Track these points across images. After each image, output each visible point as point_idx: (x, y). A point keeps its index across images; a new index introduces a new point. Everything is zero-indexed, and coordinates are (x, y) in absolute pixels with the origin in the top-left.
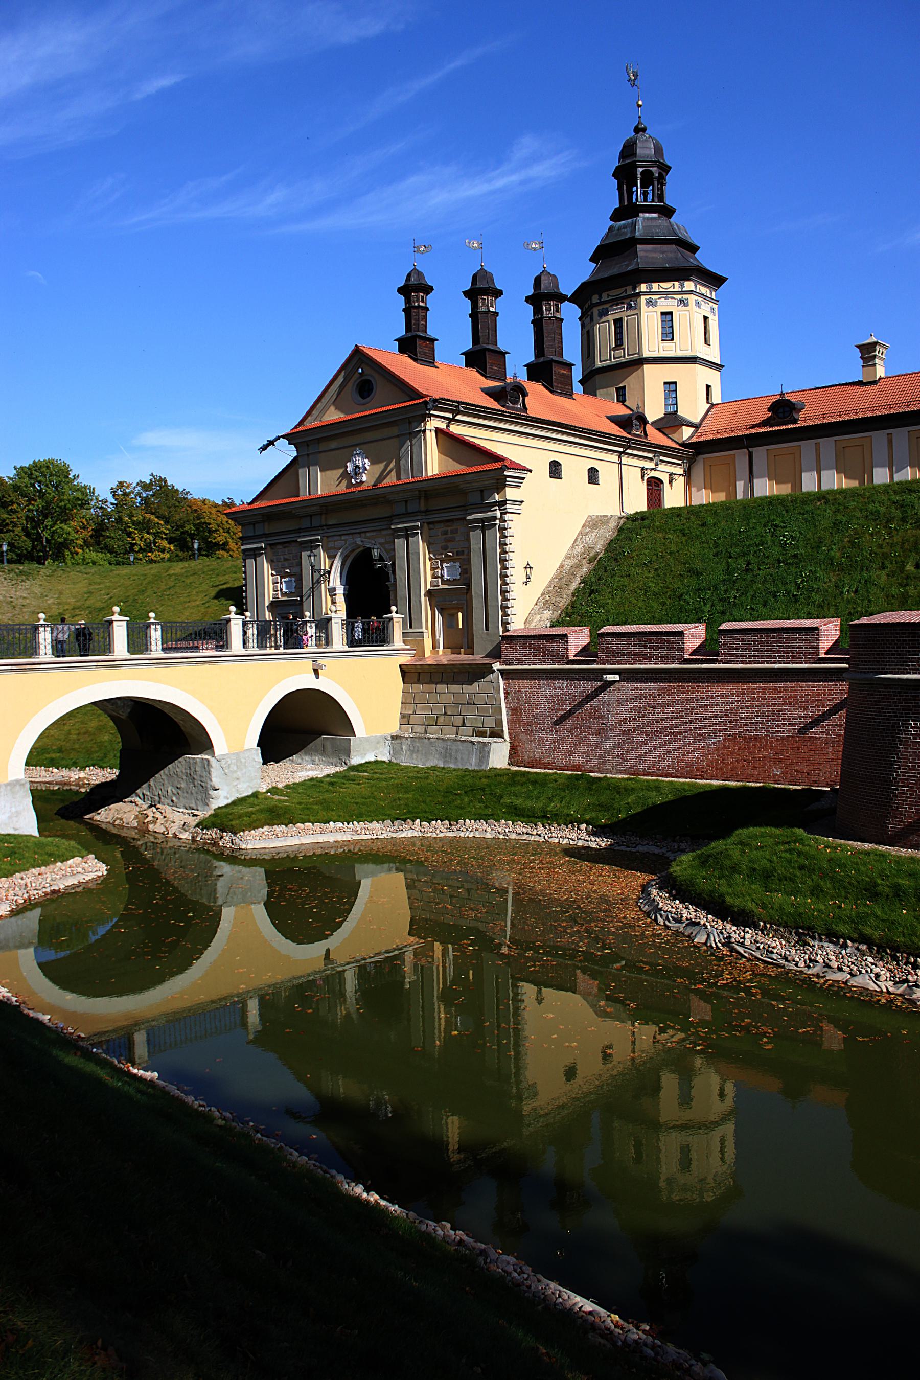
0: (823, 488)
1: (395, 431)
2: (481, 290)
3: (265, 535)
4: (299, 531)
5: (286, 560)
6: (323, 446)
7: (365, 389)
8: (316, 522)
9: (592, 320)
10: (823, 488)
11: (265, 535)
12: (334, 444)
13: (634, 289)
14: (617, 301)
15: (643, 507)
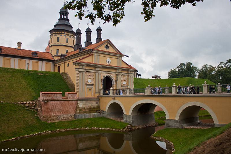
0: (43, 71)
1: (116, 57)
2: (89, 32)
3: (86, 69)
4: (95, 70)
5: (90, 75)
6: (100, 55)
7: (107, 47)
8: (99, 69)
9: (61, 35)
10: (43, 71)
11: (86, 69)
12: (103, 55)
13: (71, 34)
14: (68, 35)
15: (27, 69)
